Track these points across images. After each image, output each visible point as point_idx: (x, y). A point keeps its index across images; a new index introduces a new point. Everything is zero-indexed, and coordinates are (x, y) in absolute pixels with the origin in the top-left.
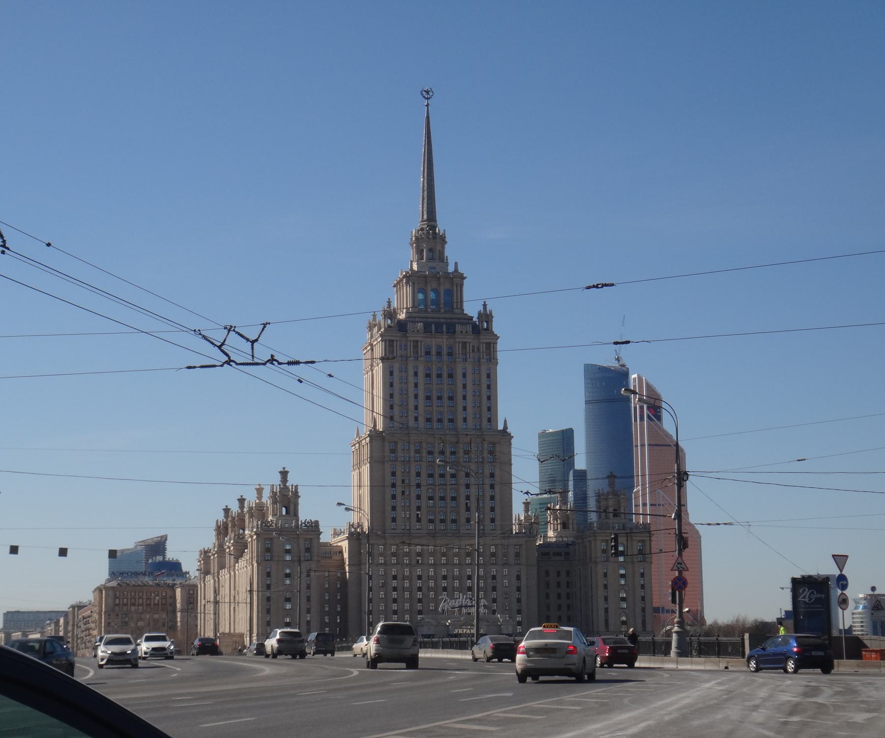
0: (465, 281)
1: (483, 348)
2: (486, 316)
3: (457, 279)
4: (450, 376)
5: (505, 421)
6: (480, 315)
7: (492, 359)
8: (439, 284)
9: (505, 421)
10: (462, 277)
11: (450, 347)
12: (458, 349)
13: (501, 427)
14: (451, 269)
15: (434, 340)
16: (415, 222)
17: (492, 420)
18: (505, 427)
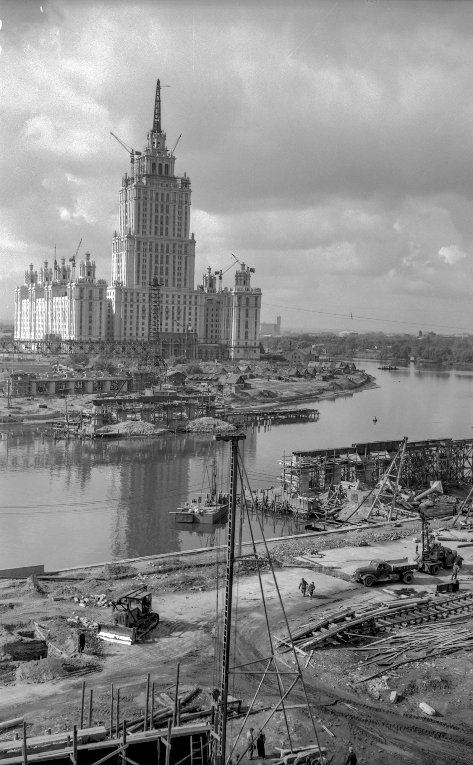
7: (188, 203)
10: (175, 159)
11: (168, 195)
18: (193, 237)
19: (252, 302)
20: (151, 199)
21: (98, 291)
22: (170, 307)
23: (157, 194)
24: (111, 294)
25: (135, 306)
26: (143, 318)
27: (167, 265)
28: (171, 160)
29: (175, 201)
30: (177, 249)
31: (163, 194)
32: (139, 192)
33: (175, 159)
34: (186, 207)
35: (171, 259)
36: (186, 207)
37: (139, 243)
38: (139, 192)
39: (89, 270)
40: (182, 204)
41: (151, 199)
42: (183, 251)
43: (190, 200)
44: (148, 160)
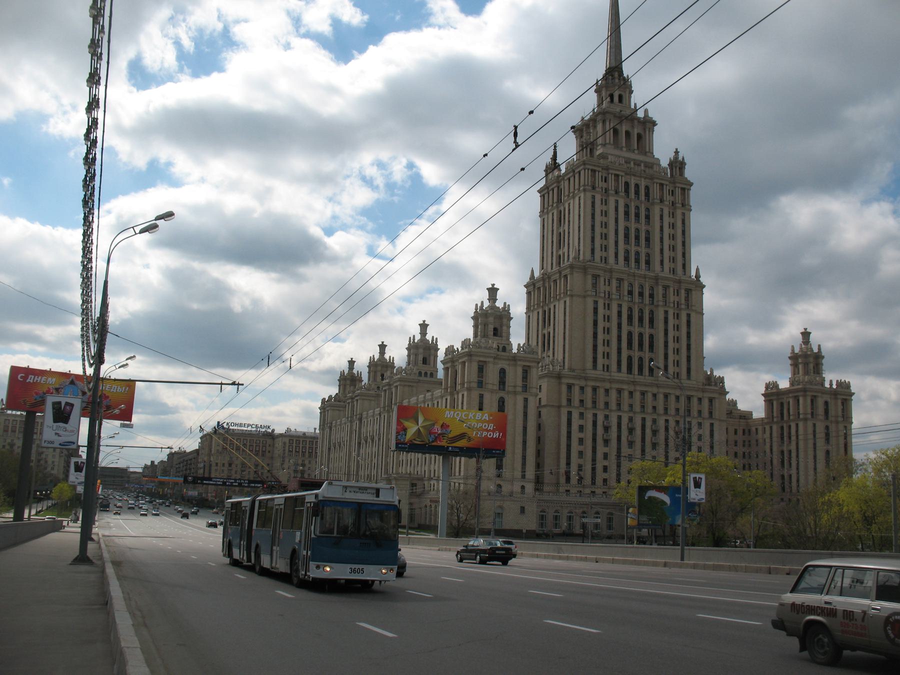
0: (655, 128)
1: (678, 192)
2: (677, 164)
3: (648, 124)
4: (648, 217)
5: (698, 270)
6: (671, 164)
7: (686, 206)
8: (633, 127)
9: (698, 270)
10: (654, 124)
11: (647, 188)
12: (655, 192)
13: (693, 273)
14: (640, 114)
15: (633, 178)
16: (598, 68)
17: (685, 266)
18: (698, 276)
19: (836, 409)
20: (617, 192)
21: (520, 371)
22: (661, 423)
23: (627, 184)
24: (544, 390)
25: (589, 416)
26: (606, 442)
27: (652, 331)
28: (648, 125)
29: (662, 201)
30: (672, 298)
31: (637, 186)
32: (594, 176)
33: (654, 124)
34: (684, 214)
35: (660, 315)
36: (684, 214)
37: (596, 277)
38: (594, 176)
39: (497, 326)
40: (675, 208)
41: (617, 192)
42: (683, 301)
43: (689, 201)
44: (604, 122)
